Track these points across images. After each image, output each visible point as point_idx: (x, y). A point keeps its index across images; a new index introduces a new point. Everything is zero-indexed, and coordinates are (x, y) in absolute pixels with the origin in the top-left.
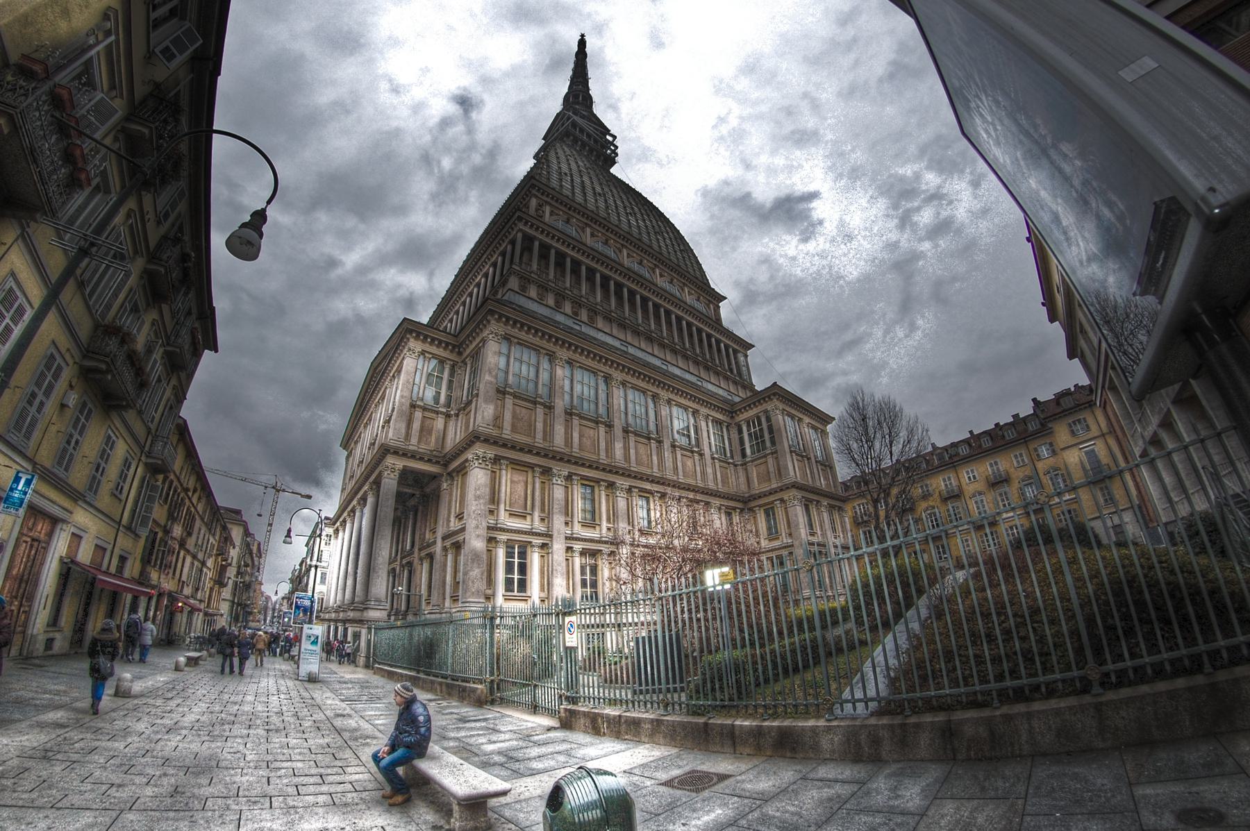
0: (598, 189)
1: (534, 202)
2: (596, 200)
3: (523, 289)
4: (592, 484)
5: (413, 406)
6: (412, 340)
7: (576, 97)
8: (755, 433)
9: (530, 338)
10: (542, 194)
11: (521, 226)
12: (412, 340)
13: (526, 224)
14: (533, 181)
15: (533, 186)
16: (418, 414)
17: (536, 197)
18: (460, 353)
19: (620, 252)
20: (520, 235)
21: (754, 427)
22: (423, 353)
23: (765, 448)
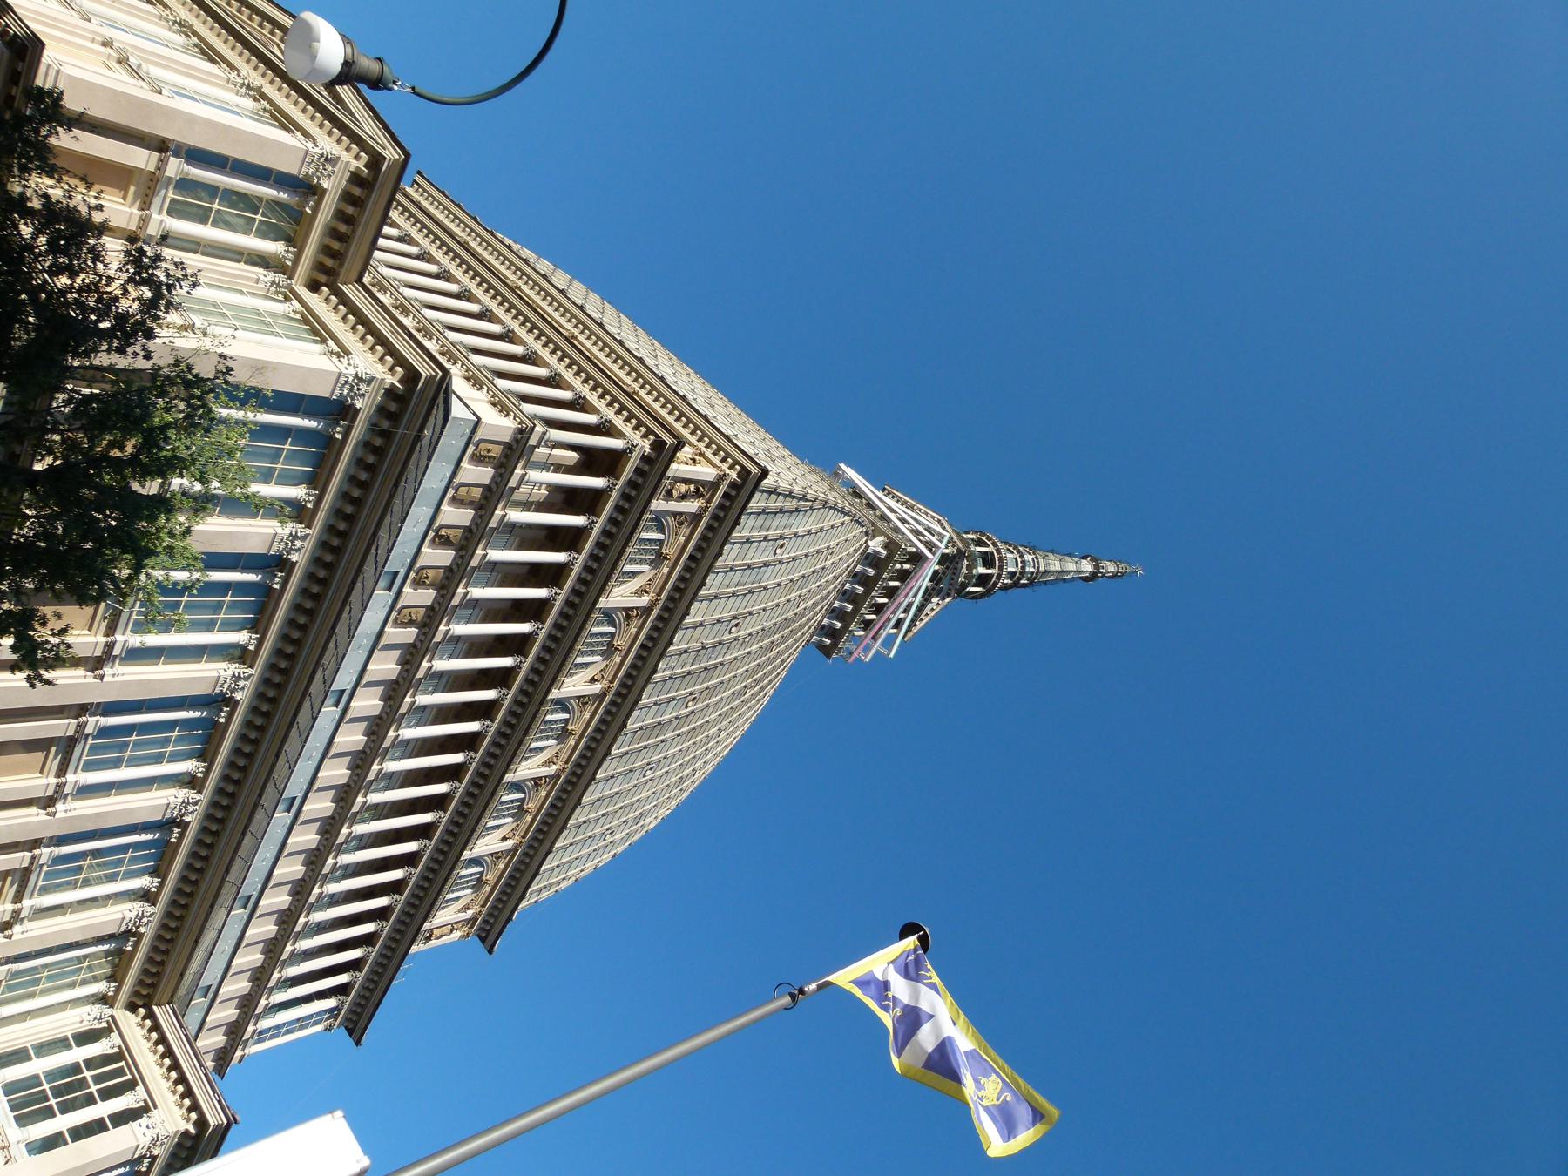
1: (705, 472)
8: (82, 1083)
18: (314, 287)
19: (593, 680)
21: (98, 1079)
23: (22, 1121)
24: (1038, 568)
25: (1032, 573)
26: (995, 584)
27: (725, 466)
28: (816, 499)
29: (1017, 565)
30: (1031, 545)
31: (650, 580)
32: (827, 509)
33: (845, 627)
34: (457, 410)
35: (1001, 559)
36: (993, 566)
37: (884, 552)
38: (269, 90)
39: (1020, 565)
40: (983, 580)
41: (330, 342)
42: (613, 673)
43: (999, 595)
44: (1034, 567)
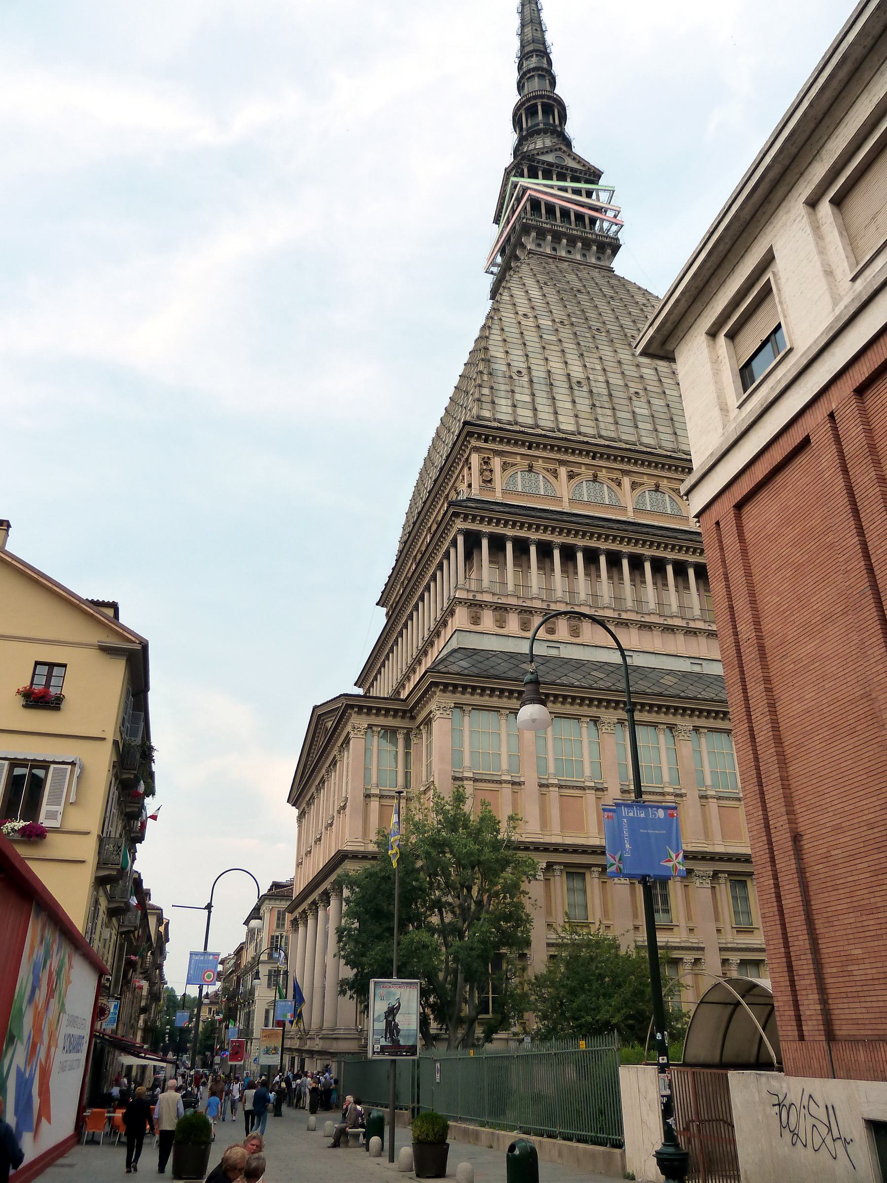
0: (577, 372)
2: (574, 402)
3: (476, 620)
4: (582, 871)
5: (368, 796)
6: (354, 715)
7: (532, 112)
9: (486, 700)
10: (486, 441)
11: (459, 524)
12: (354, 715)
13: (465, 519)
14: (468, 428)
15: (470, 434)
16: (374, 804)
17: (477, 449)
18: (413, 718)
19: (619, 484)
20: (460, 540)
22: (370, 726)
24: (532, 51)
25: (537, 56)
26: (549, 97)
27: (470, 446)
28: (483, 360)
29: (533, 76)
30: (517, 61)
31: (548, 471)
32: (491, 342)
33: (594, 241)
34: (454, 645)
35: (528, 100)
36: (536, 105)
37: (533, 234)
38: (339, 743)
39: (532, 74)
40: (548, 110)
41: (431, 716)
42: (615, 472)
43: (560, 91)
44: (532, 56)
